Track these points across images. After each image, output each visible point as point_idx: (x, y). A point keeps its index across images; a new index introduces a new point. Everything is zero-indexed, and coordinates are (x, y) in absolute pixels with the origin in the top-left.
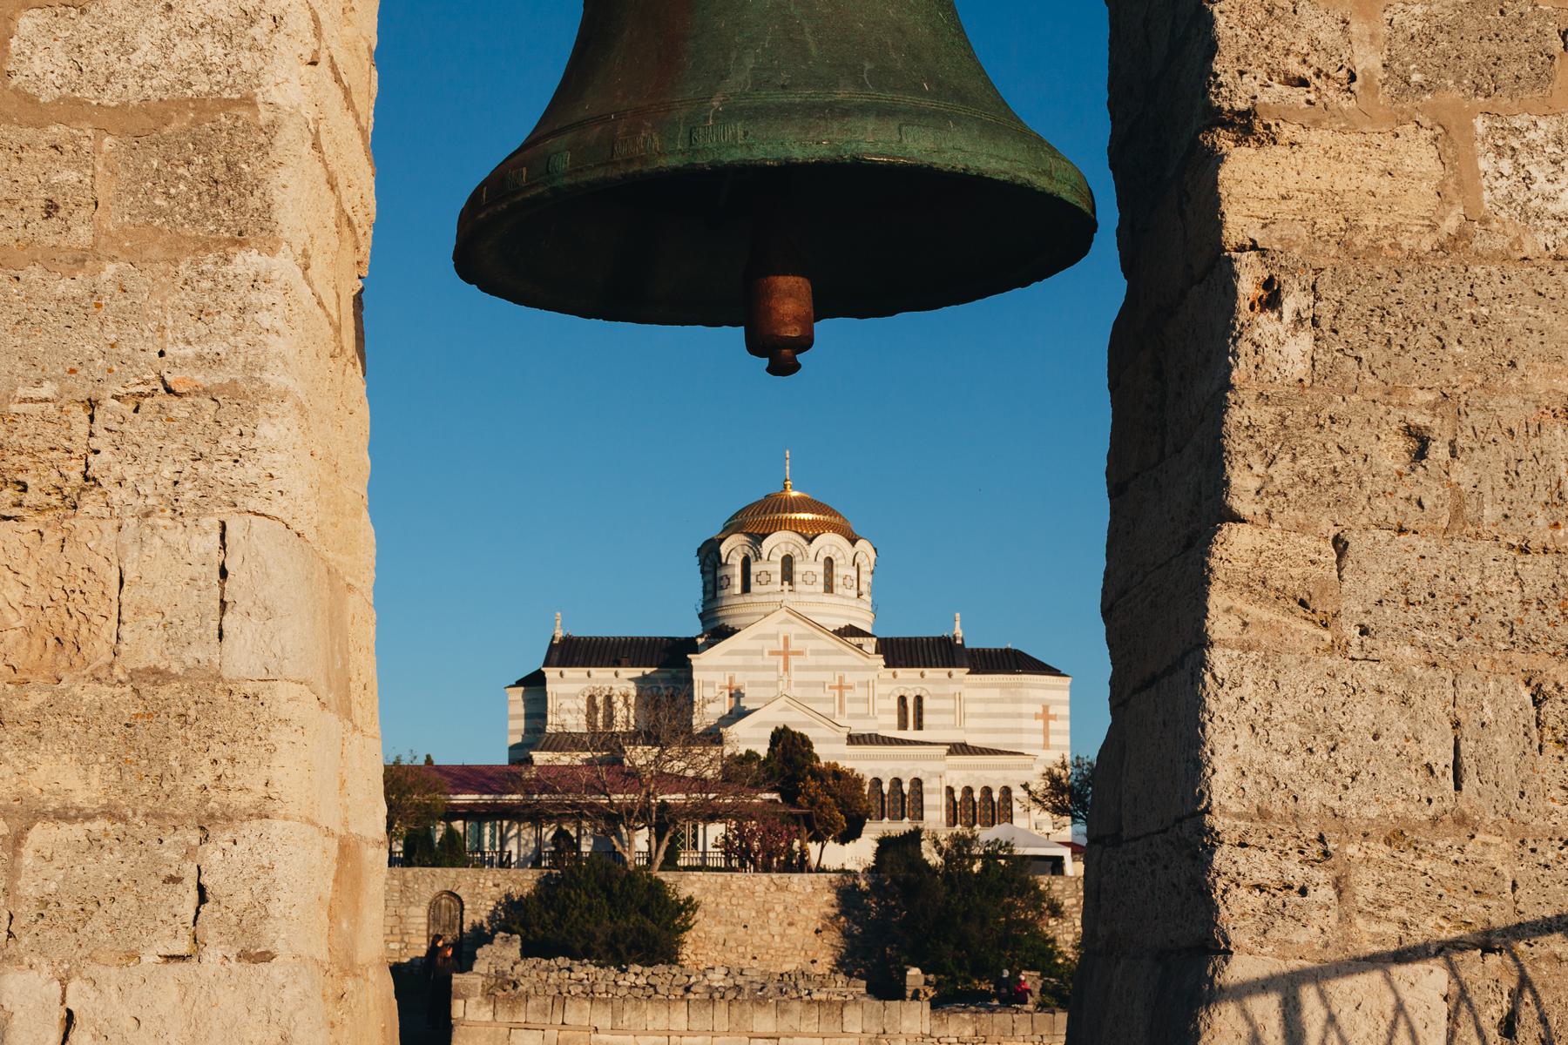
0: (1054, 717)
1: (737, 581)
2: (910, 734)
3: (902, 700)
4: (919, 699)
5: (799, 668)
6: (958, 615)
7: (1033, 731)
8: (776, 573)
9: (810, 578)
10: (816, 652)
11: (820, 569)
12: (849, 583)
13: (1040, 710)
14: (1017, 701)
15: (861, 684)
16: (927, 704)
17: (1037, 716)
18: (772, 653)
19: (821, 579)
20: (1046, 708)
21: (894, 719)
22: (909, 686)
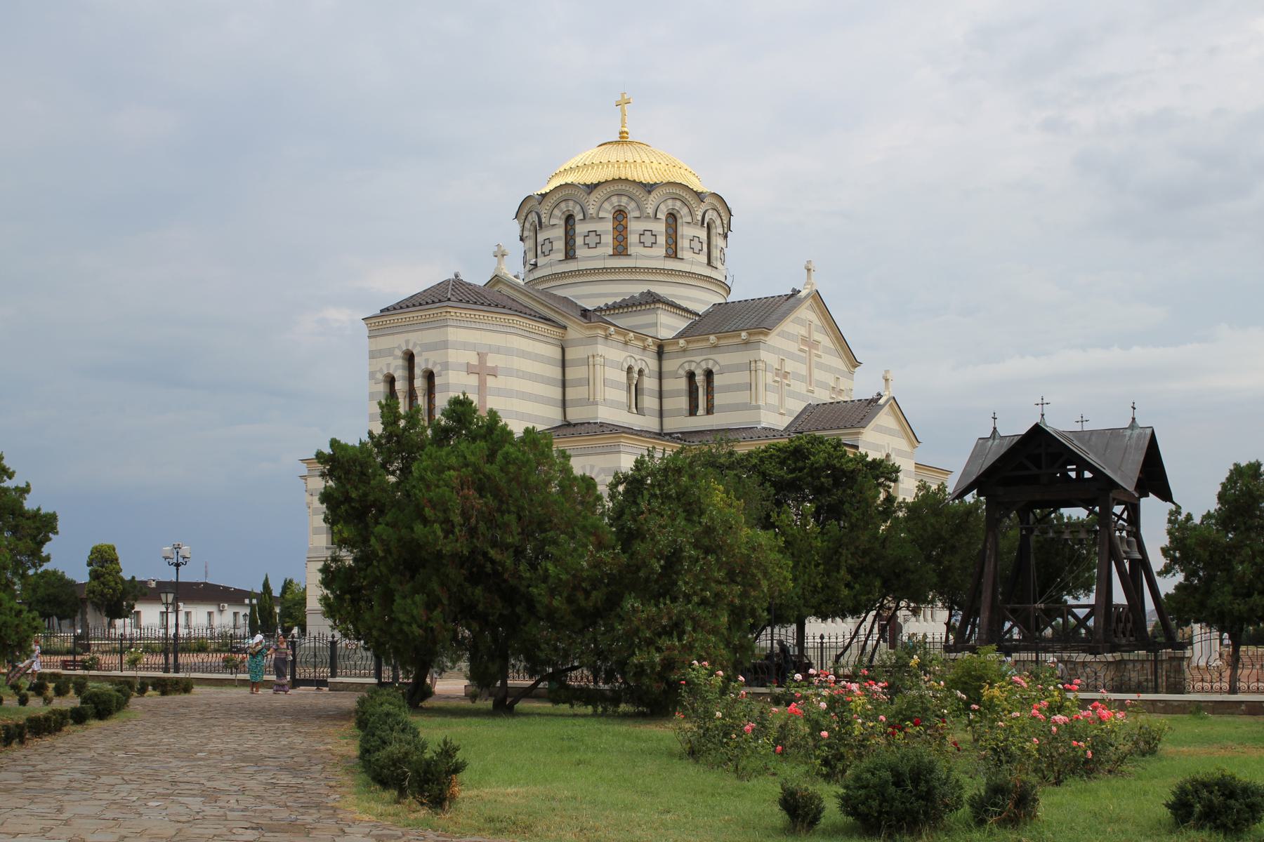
1: (530, 255)
2: (702, 421)
3: (691, 376)
4: (709, 374)
8: (559, 238)
9: (592, 240)
11: (607, 227)
12: (648, 239)
16: (718, 380)
19: (608, 239)
21: (683, 402)
22: (698, 359)
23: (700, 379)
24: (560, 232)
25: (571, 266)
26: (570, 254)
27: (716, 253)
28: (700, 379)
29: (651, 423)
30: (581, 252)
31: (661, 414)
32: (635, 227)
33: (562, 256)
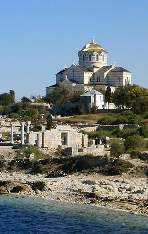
0: (121, 79)
2: (98, 83)
3: (97, 77)
4: (99, 77)
5: (75, 74)
6: (114, 63)
7: (117, 81)
10: (77, 71)
12: (94, 58)
13: (118, 78)
14: (115, 77)
15: (82, 76)
16: (100, 78)
17: (118, 79)
18: (72, 72)
20: (119, 77)
23: (98, 78)
24: (82, 57)
25: (84, 61)
26: (84, 60)
27: (104, 59)
28: (98, 78)
29: (93, 83)
30: (85, 60)
31: (94, 82)
32: (92, 57)
33: (83, 60)
